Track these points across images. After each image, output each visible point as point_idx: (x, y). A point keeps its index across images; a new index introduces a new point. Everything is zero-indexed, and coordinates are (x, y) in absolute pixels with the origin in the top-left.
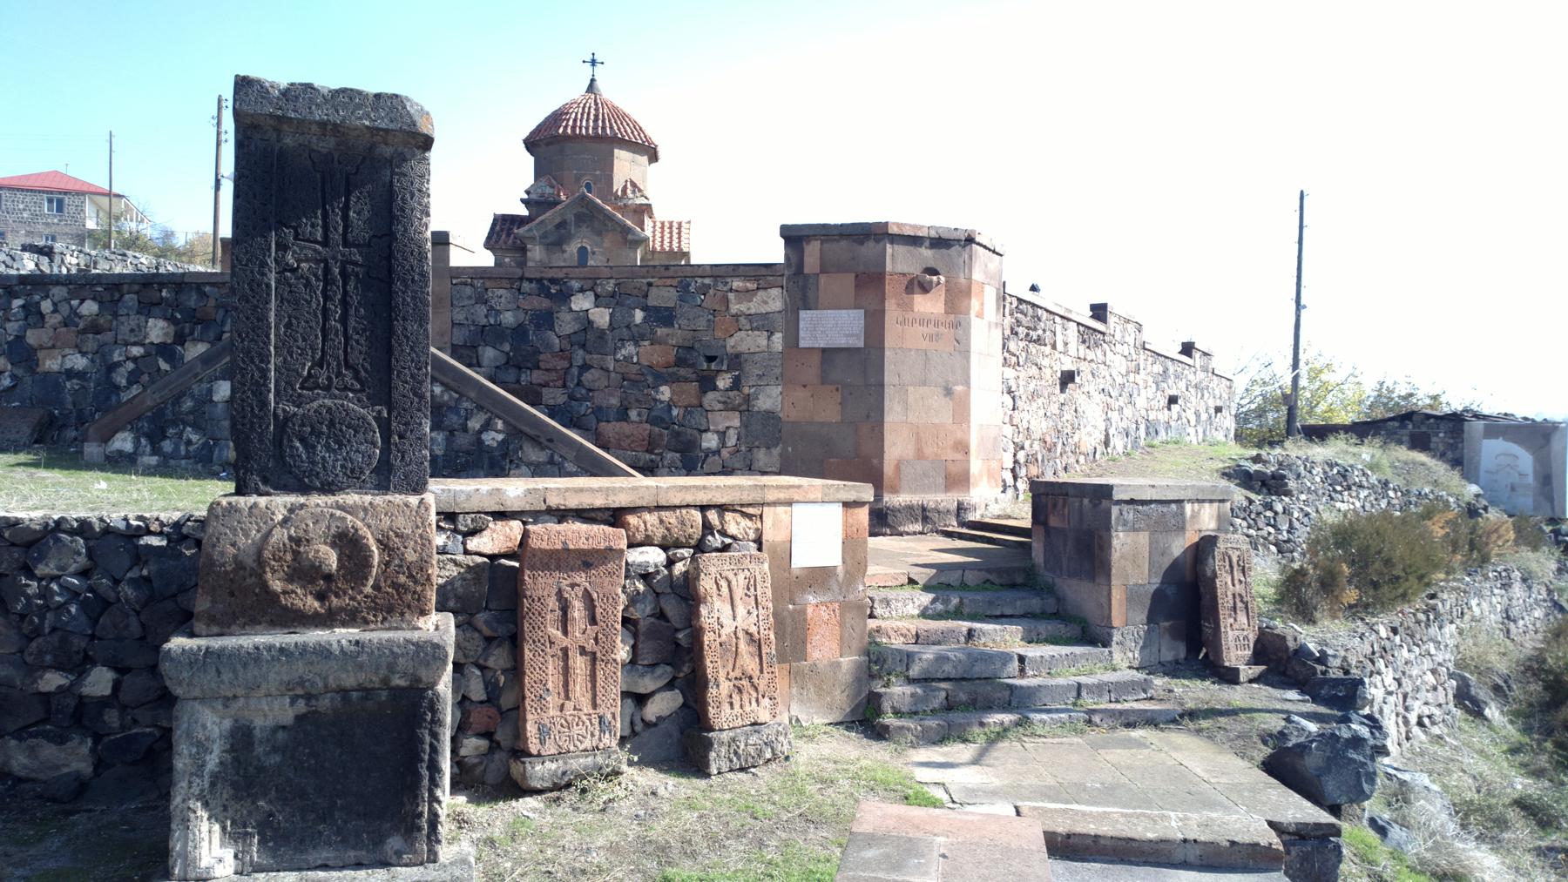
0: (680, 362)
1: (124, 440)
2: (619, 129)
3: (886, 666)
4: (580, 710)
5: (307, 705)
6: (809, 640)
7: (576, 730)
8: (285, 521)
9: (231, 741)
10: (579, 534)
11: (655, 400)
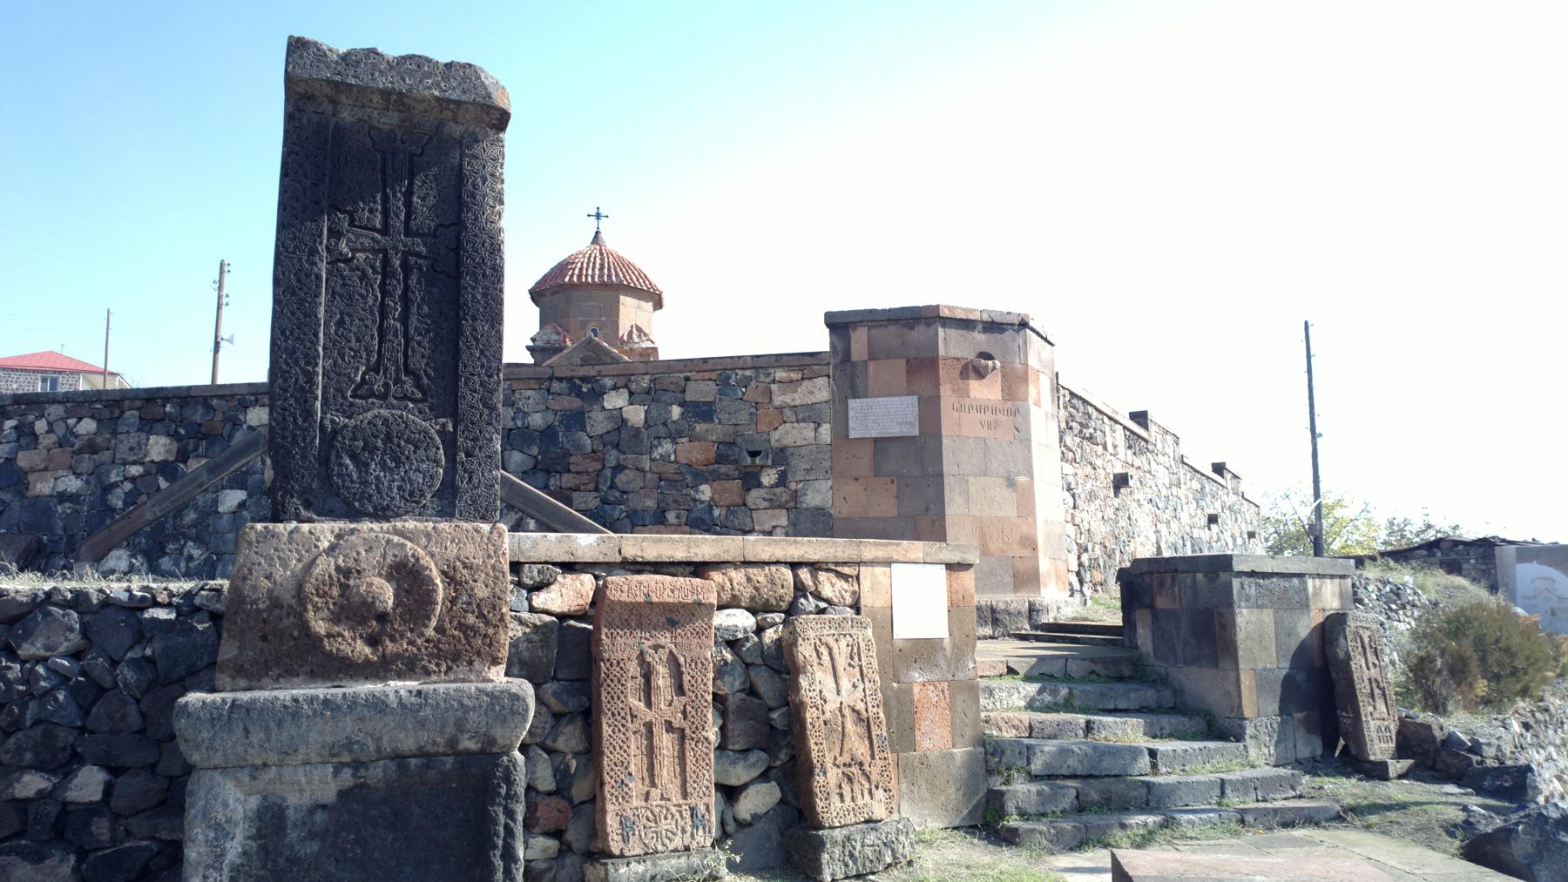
0: (721, 459)
1: (118, 558)
2: (624, 277)
3: (1004, 760)
4: (669, 800)
5: (354, 775)
6: (917, 726)
7: (664, 825)
8: (332, 548)
9: (258, 824)
10: (662, 588)
11: (695, 500)
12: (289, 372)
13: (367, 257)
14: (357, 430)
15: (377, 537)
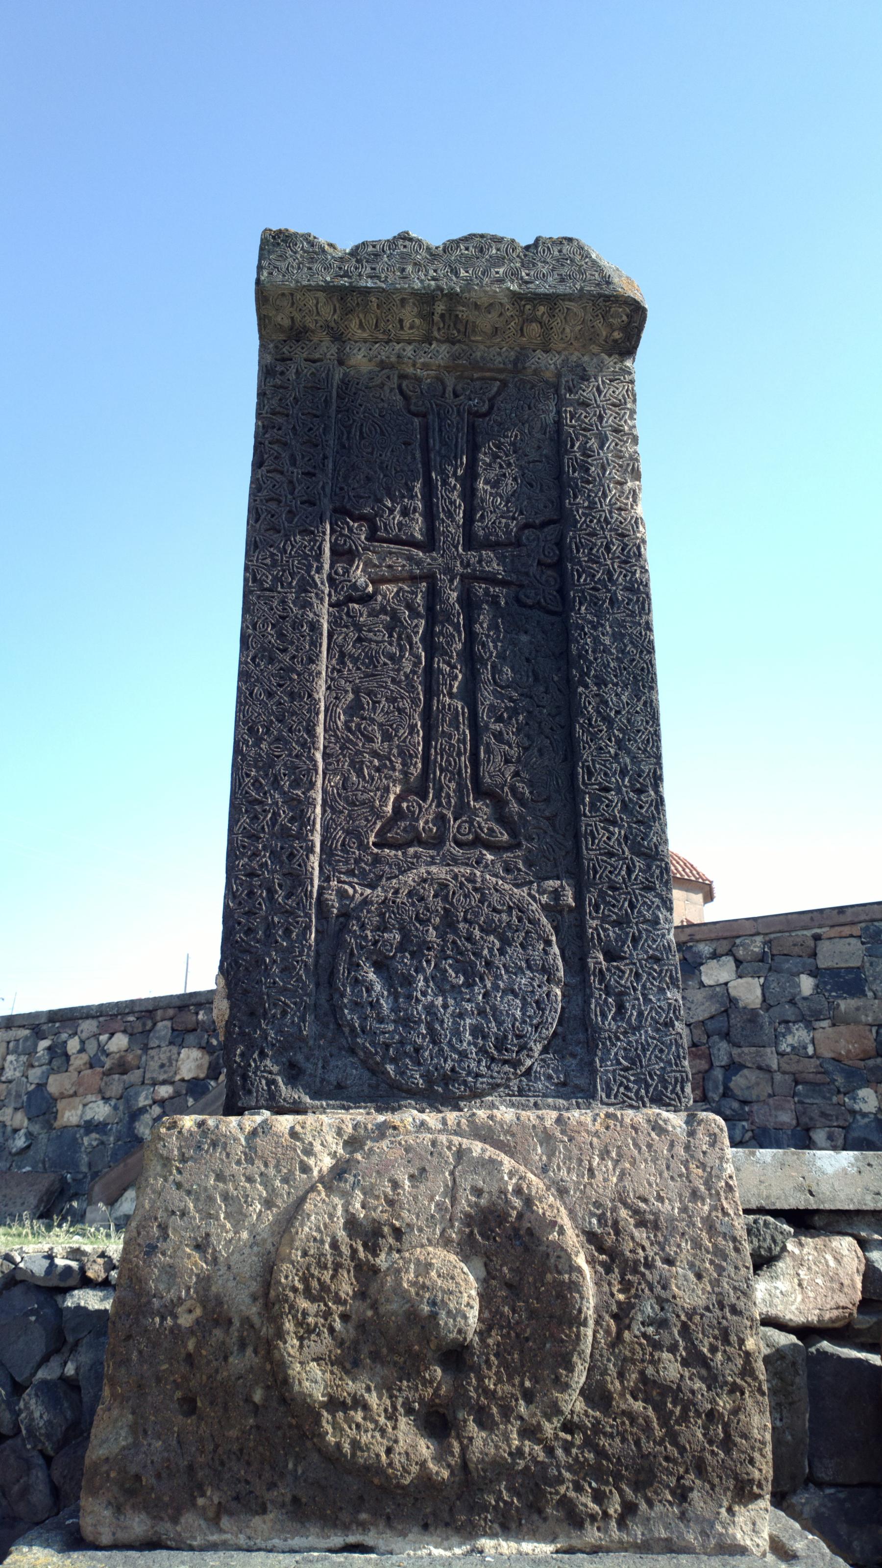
8: (340, 1171)
11: (853, 1112)
12: (261, 803)
13: (401, 589)
14: (388, 907)
15: (434, 1143)
